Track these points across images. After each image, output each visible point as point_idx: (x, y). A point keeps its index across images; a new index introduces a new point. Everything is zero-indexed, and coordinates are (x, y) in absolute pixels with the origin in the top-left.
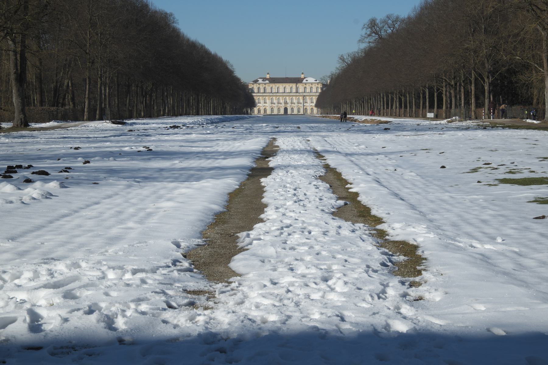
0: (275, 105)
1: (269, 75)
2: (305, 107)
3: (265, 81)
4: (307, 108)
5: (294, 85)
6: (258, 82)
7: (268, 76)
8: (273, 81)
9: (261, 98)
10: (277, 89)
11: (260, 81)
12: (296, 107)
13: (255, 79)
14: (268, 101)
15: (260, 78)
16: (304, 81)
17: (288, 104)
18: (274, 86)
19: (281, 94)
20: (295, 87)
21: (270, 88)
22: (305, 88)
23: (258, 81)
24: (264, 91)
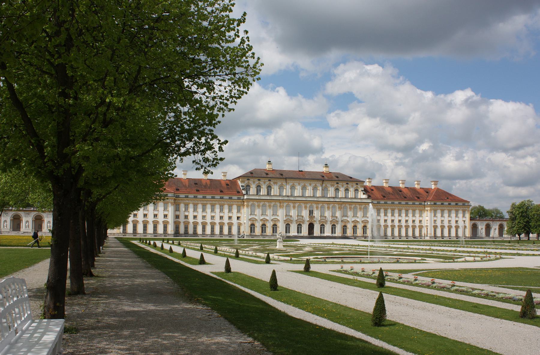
5: (319, 184)
18: (284, 183)
20: (320, 188)
24: (268, 192)
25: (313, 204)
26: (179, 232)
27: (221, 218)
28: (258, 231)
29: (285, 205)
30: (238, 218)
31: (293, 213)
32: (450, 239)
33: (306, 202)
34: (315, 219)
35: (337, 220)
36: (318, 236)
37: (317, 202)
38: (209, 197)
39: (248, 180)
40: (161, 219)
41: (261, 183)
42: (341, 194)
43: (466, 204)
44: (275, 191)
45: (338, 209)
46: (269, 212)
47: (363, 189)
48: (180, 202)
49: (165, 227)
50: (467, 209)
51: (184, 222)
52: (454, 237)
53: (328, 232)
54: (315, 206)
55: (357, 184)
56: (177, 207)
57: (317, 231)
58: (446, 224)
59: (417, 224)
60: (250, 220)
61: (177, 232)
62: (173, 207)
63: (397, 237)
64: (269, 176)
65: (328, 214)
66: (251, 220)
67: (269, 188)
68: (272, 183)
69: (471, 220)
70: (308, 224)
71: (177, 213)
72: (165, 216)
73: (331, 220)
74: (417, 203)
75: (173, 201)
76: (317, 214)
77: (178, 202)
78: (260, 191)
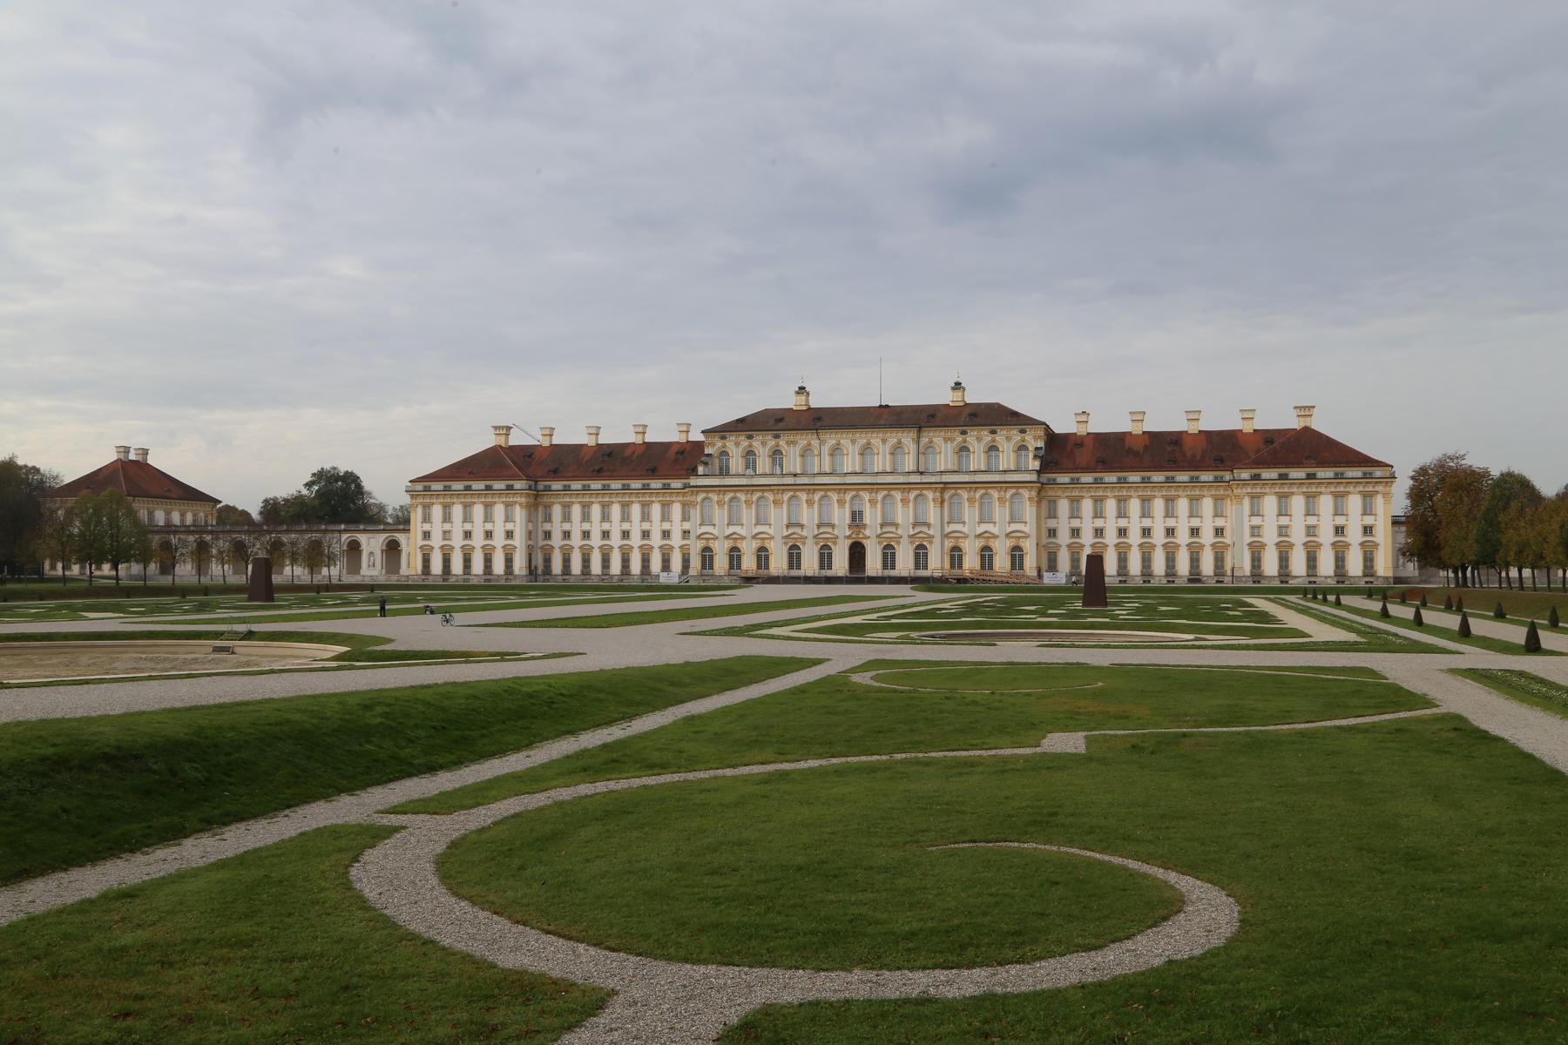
2: (949, 544)
5: (907, 438)
12: (905, 541)
18: (815, 443)
20: (912, 447)
25: (861, 493)
26: (551, 571)
28: (721, 564)
29: (786, 496)
30: (686, 533)
31: (808, 516)
32: (1315, 582)
33: (842, 488)
34: (867, 532)
35: (931, 532)
36: (874, 575)
37: (873, 487)
38: (616, 484)
39: (723, 438)
40: (499, 540)
41: (756, 444)
42: (977, 460)
43: (1378, 473)
44: (793, 462)
45: (932, 504)
46: (748, 515)
47: (1041, 444)
48: (552, 500)
49: (509, 561)
50: (1380, 488)
51: (561, 548)
52: (1326, 577)
54: (866, 496)
55: (1023, 431)
56: (546, 513)
57: (873, 565)
58: (1298, 537)
59: (1207, 537)
60: (699, 537)
61: (532, 571)
62: (524, 512)
63: (1137, 579)
64: (781, 425)
65: (903, 515)
66: (703, 539)
67: (776, 454)
68: (782, 443)
71: (547, 527)
72: (509, 535)
73: (912, 533)
74: (1207, 476)
76: (871, 517)
77: (549, 500)
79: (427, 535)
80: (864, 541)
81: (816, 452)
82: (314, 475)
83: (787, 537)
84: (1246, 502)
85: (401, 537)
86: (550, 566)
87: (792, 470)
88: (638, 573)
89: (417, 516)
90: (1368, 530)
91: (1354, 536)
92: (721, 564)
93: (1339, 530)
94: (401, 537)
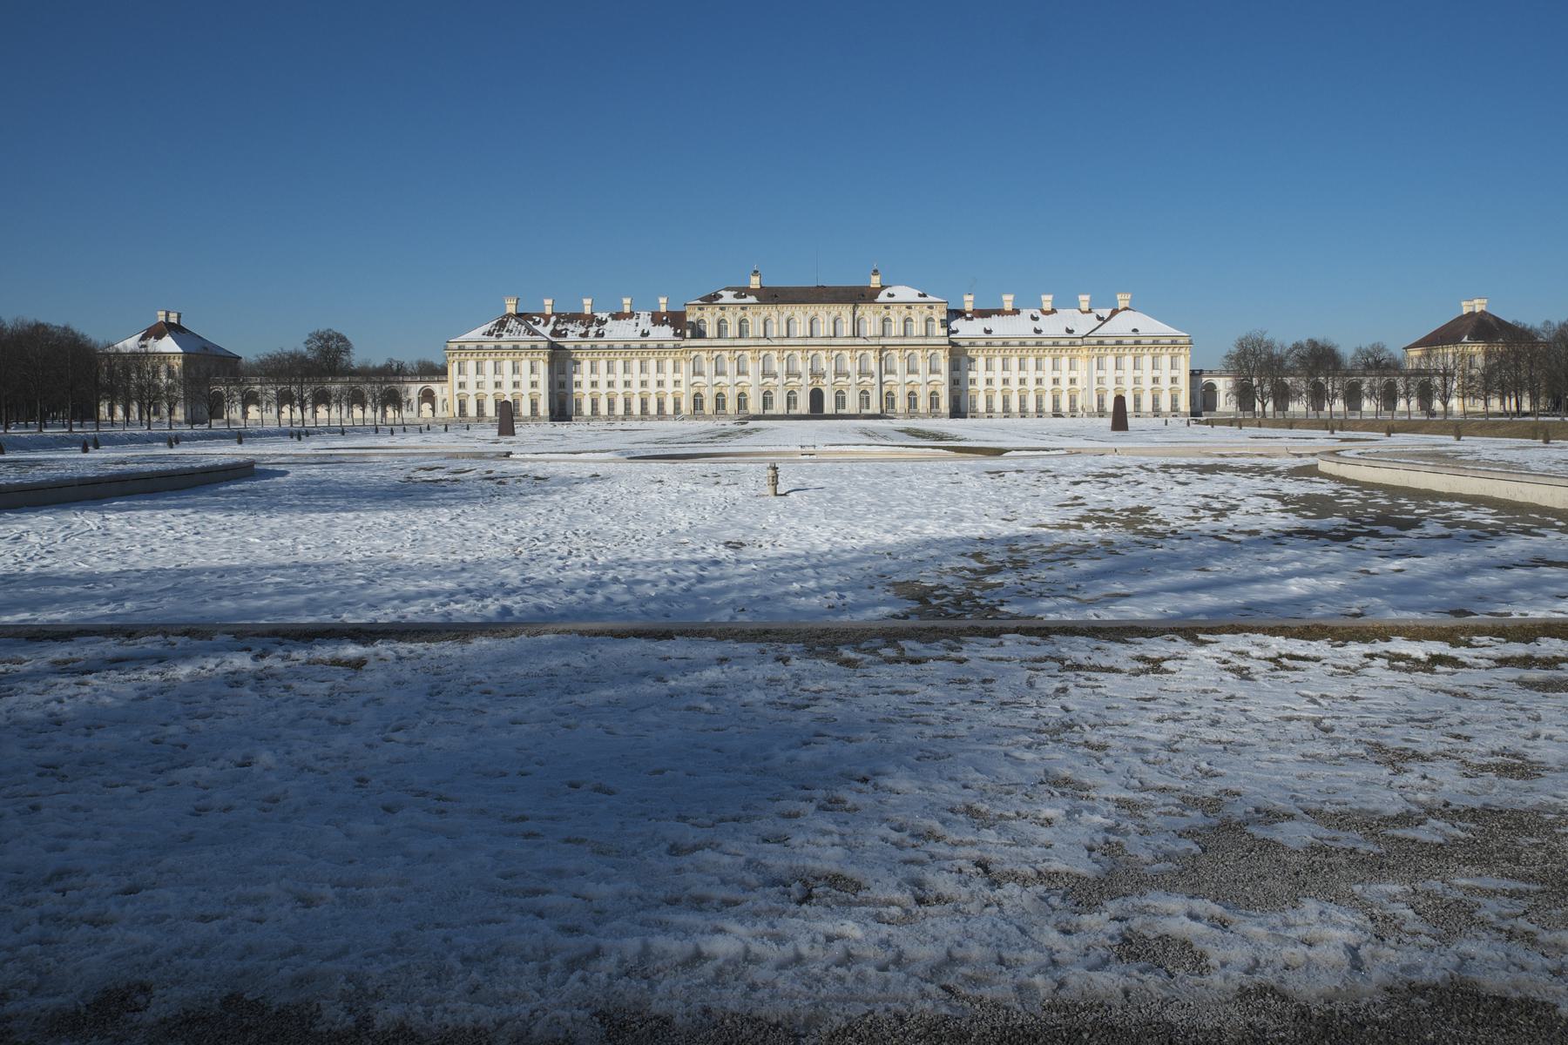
0: (776, 382)
1: (758, 279)
2: (885, 390)
3: (745, 297)
4: (894, 391)
5: (845, 311)
6: (720, 301)
7: (755, 282)
8: (770, 296)
9: (726, 354)
10: (785, 326)
11: (728, 297)
13: (711, 292)
14: (753, 367)
15: (727, 289)
16: (883, 297)
17: (823, 375)
18: (774, 314)
19: (801, 342)
20: (850, 318)
21: (761, 321)
22: (885, 320)
23: (721, 296)
27: (643, 384)
30: (677, 383)
45: (873, 360)
53: (852, 406)
57: (829, 406)
59: (1064, 385)
60: (692, 385)
62: (547, 365)
69: (1191, 375)
70: (810, 388)
71: (562, 378)
72: (534, 384)
75: (546, 357)
78: (726, 328)
79: (462, 385)
80: (822, 388)
81: (775, 321)
82: (310, 335)
83: (763, 385)
84: (1095, 360)
85: (436, 387)
86: (564, 409)
87: (757, 335)
88: (639, 413)
89: (453, 369)
90: (1174, 380)
91: (1165, 384)
92: (709, 405)
93: (1155, 380)
94: (436, 387)
